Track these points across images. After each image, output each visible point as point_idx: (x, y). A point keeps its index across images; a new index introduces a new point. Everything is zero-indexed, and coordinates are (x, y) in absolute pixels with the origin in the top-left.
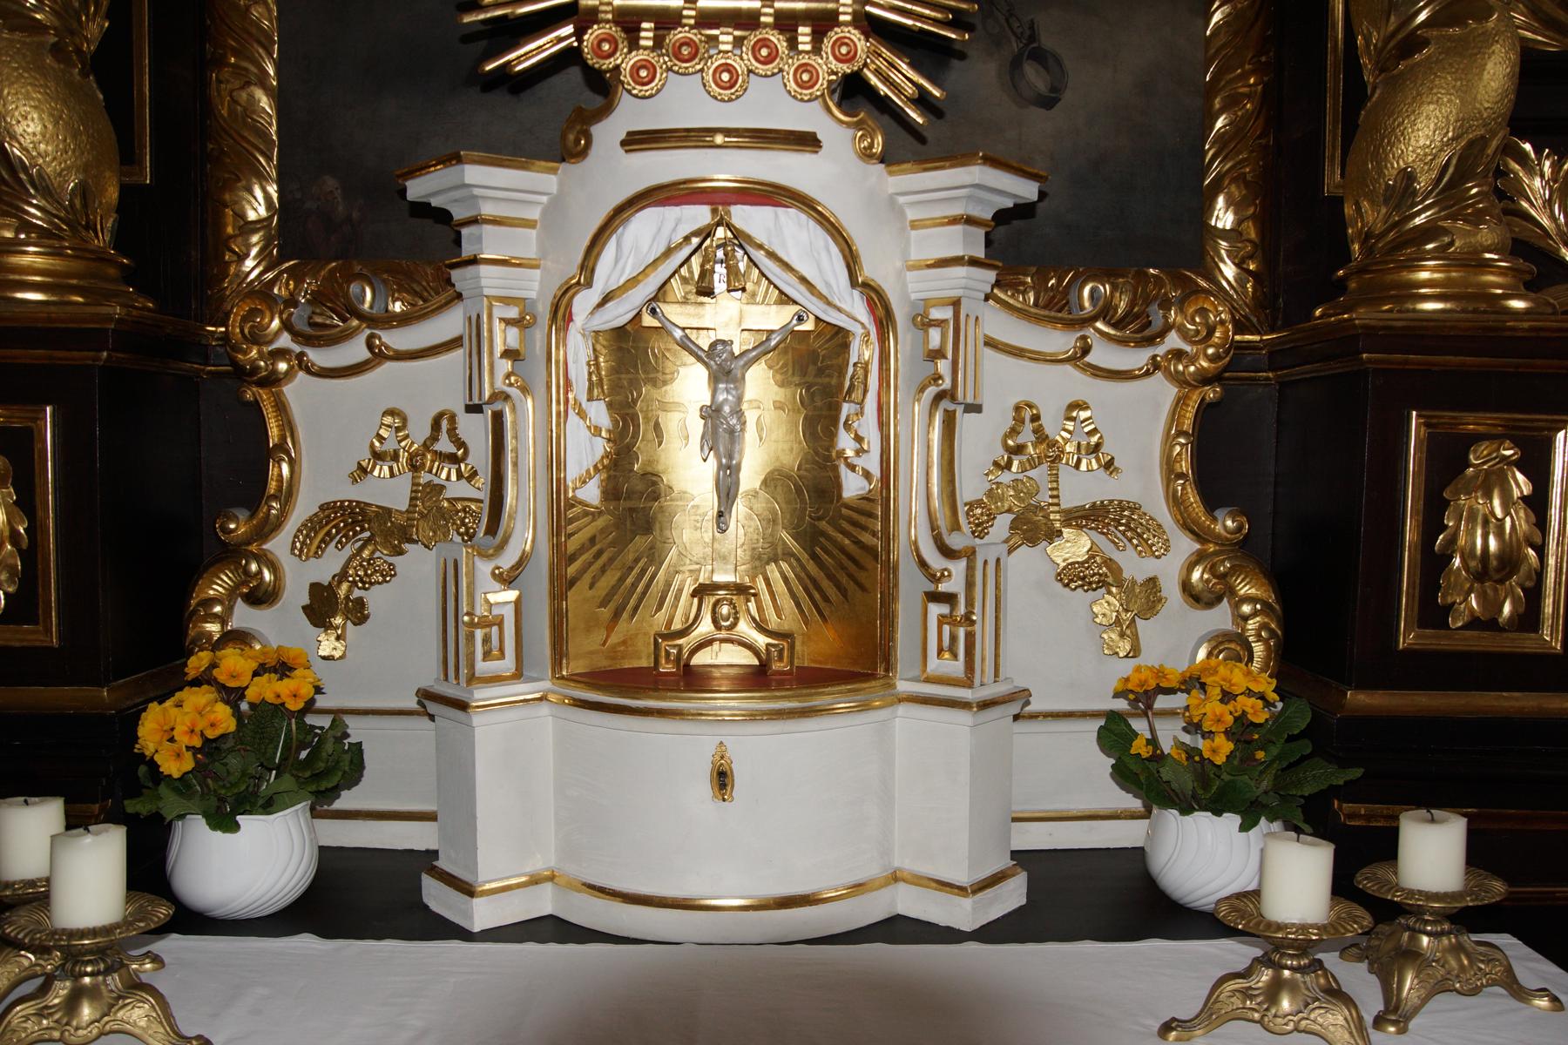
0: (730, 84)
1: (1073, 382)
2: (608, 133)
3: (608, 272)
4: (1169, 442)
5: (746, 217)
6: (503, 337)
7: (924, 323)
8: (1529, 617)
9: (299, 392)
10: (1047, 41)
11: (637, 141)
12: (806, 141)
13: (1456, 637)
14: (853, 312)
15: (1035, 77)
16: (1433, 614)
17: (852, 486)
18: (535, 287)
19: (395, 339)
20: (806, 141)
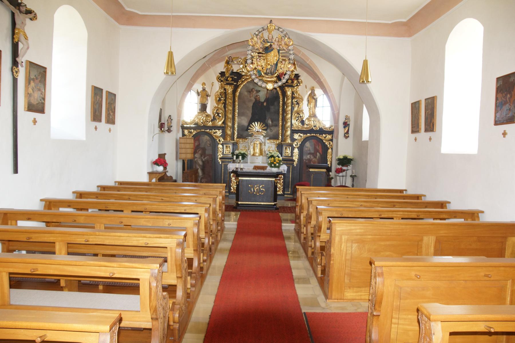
0: (258, 135)
1: (271, 145)
2: (254, 136)
3: (254, 141)
4: (275, 147)
5: (259, 139)
6: (249, 143)
7: (264, 143)
8: (289, 155)
9: (239, 144)
10: (272, 129)
11: (255, 137)
12: (260, 137)
13: (286, 155)
14: (262, 143)
15: (271, 131)
16: (285, 154)
17: (262, 149)
18: (251, 141)
19: (244, 143)
20: (260, 137)
